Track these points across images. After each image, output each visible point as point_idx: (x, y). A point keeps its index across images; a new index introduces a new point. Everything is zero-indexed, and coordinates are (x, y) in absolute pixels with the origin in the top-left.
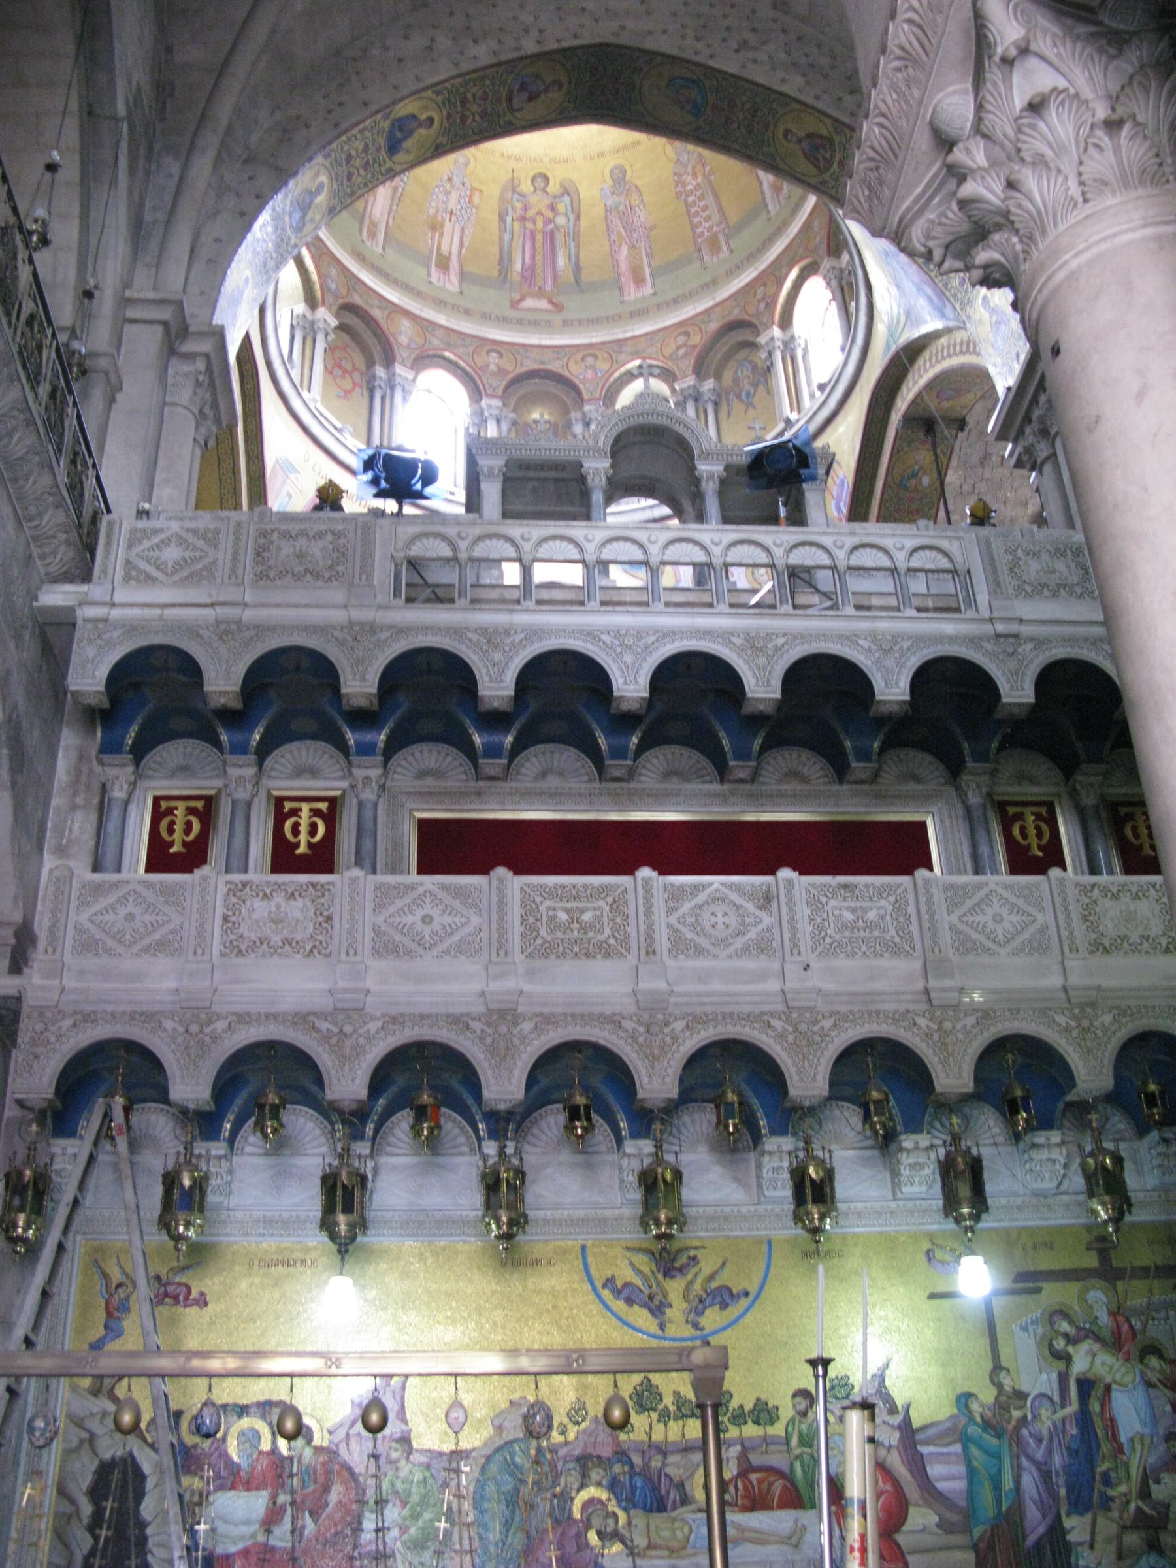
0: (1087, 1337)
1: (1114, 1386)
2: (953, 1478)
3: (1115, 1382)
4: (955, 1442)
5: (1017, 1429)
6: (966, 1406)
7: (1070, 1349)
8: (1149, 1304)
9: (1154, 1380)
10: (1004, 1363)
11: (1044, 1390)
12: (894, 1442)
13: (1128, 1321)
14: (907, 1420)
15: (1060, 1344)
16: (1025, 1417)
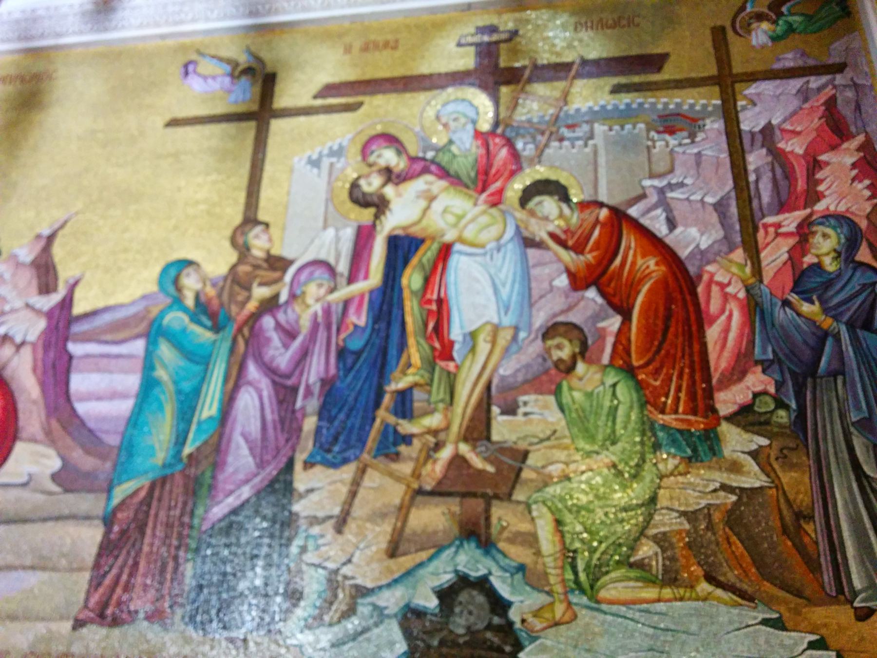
0: (425, 171)
1: (457, 247)
2: (114, 395)
3: (461, 240)
4: (137, 337)
5: (256, 317)
6: (176, 282)
7: (389, 191)
8: (557, 118)
9: (542, 234)
10: (262, 216)
11: (322, 256)
12: (32, 337)
13: (510, 143)
14: (67, 302)
15: (372, 184)
16: (276, 296)
